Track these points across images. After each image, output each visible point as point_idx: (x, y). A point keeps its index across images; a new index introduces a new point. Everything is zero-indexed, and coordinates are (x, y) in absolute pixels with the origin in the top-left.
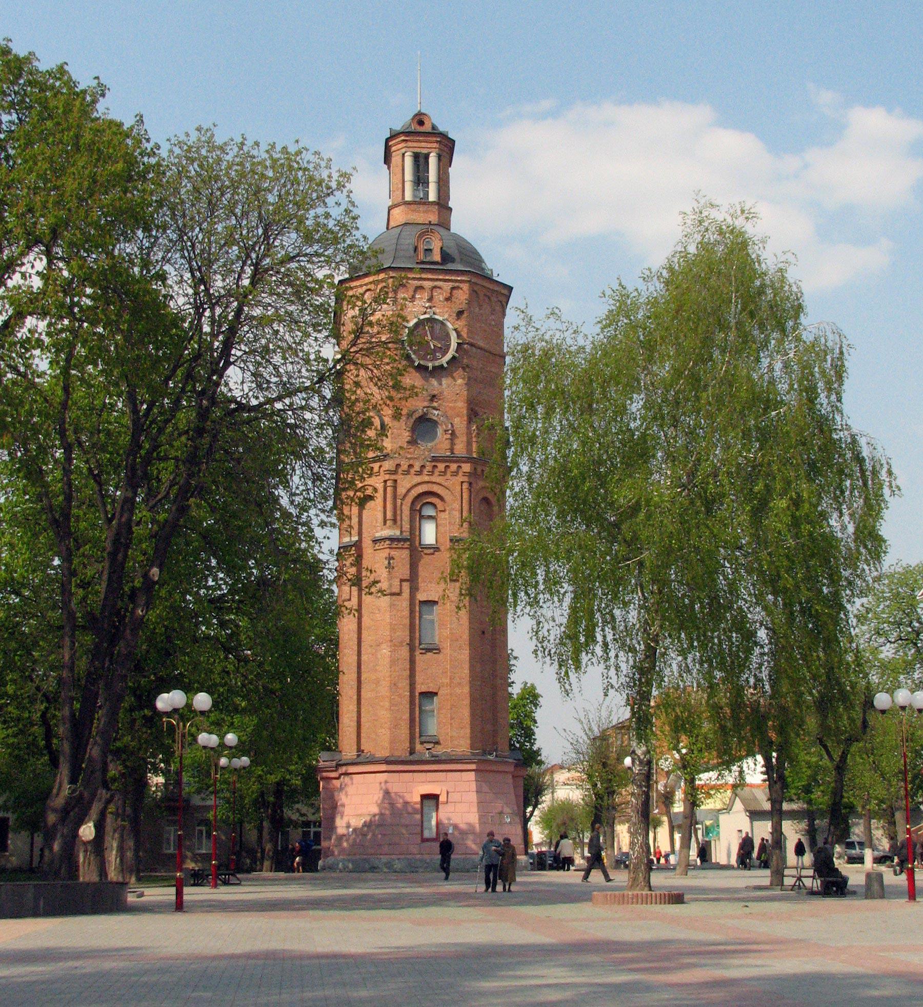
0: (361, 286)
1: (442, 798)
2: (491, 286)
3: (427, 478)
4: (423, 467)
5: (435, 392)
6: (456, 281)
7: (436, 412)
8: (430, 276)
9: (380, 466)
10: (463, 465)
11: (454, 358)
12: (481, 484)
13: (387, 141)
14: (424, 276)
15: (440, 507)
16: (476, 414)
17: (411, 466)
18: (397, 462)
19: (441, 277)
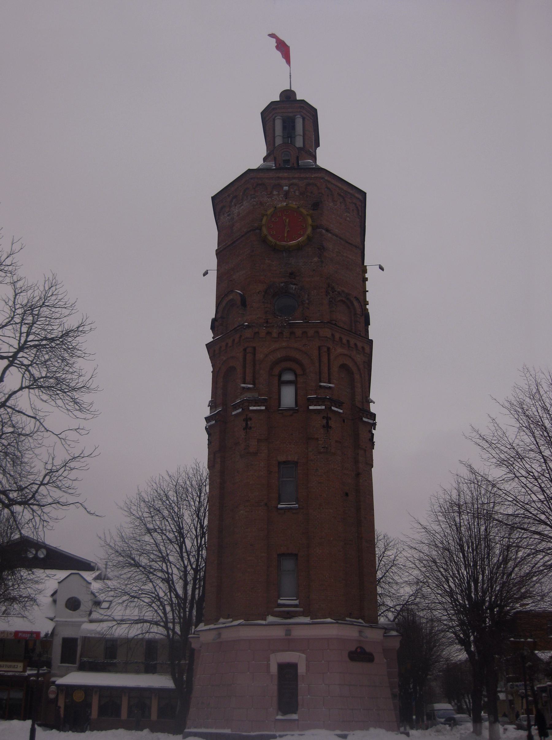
0: (229, 196)
1: (302, 669)
2: (345, 188)
3: (284, 344)
4: (281, 334)
7: (294, 287)
9: (241, 336)
11: (309, 239)
12: (340, 350)
13: (262, 113)
14: (281, 175)
17: (269, 333)
18: (257, 330)
19: (296, 176)
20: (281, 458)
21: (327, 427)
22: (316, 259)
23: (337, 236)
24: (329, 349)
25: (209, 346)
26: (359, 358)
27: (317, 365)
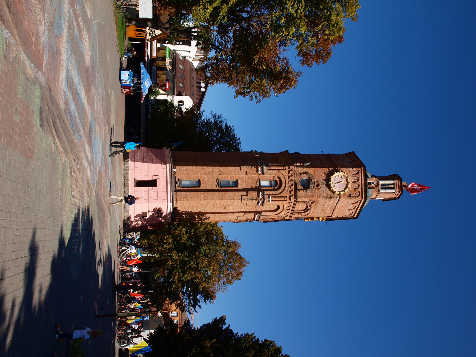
3: (287, 182)
5: (320, 186)
6: (362, 194)
7: (313, 186)
8: (363, 183)
10: (294, 197)
11: (334, 192)
12: (286, 205)
14: (363, 180)
15: (275, 188)
16: (312, 203)
20: (239, 181)
21: (253, 199)
22: (325, 195)
23: (336, 205)
24: (286, 200)
25: (287, 151)
27: (279, 195)
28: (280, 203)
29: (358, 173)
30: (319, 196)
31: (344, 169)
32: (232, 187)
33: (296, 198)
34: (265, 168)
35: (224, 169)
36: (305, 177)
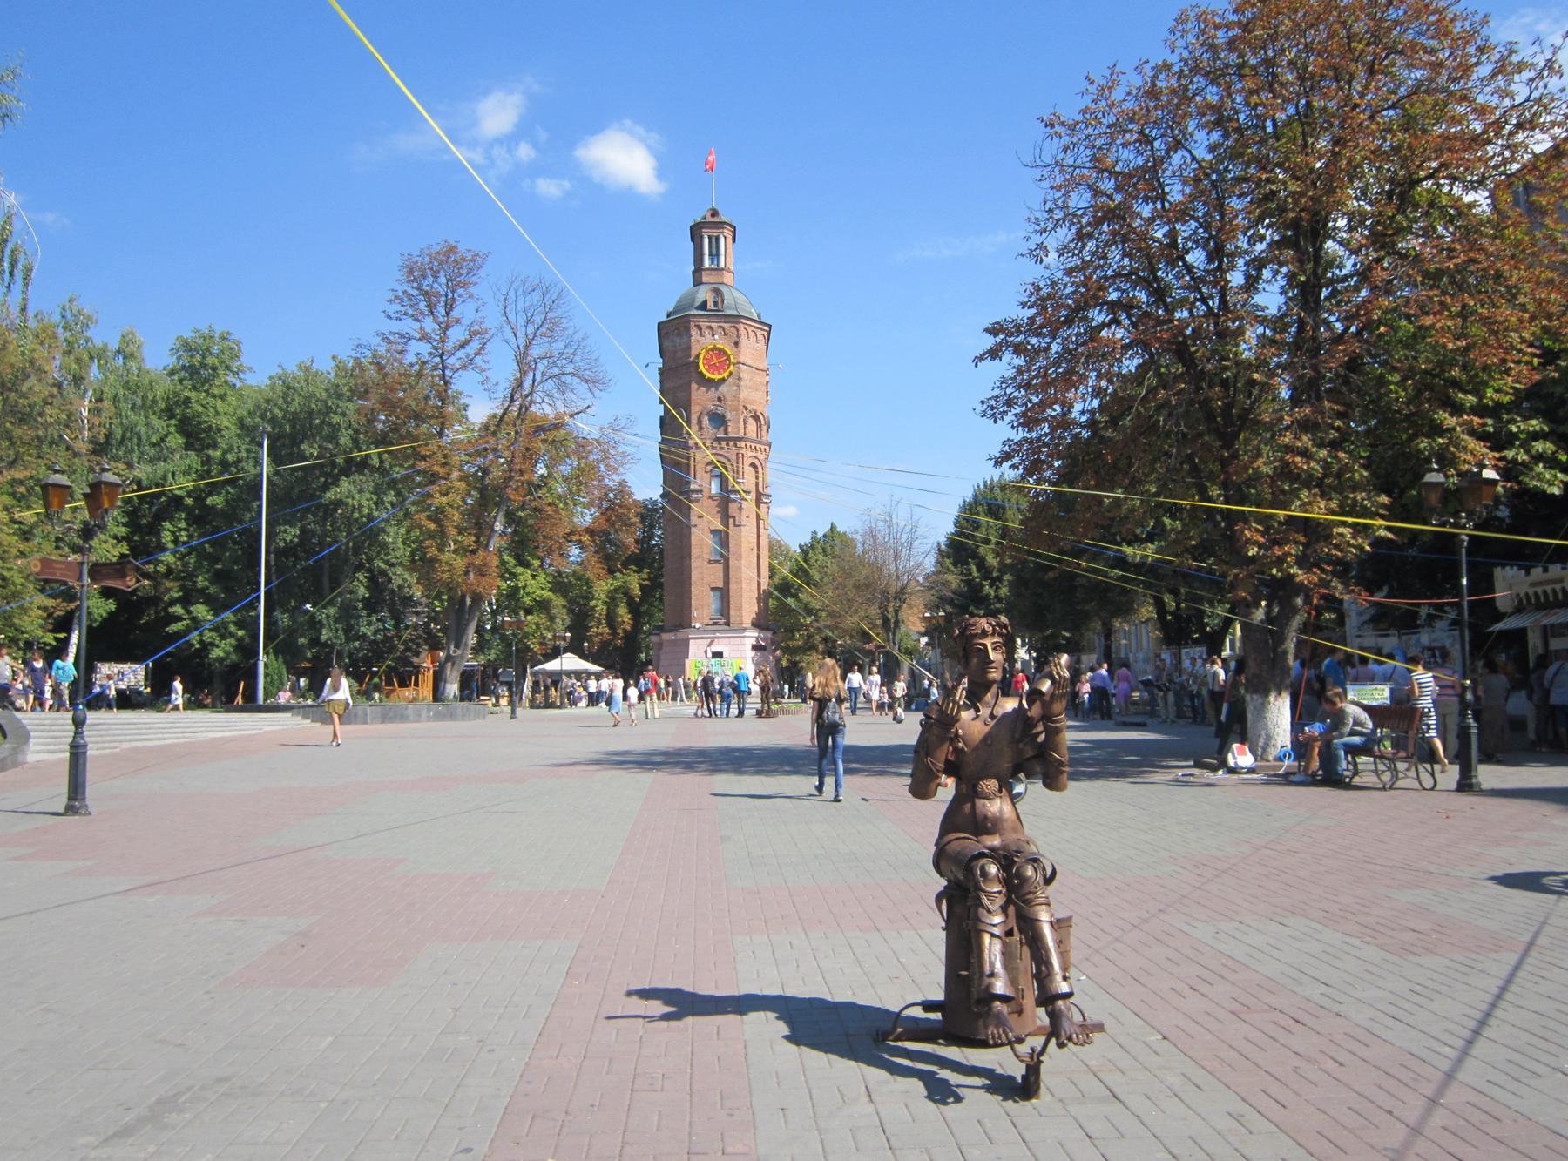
21: (740, 508)
26: (762, 457)
28: (748, 461)
29: (700, 328)
30: (736, 398)
31: (694, 352)
32: (723, 538)
33: (740, 439)
34: (692, 487)
35: (694, 552)
36: (706, 421)
